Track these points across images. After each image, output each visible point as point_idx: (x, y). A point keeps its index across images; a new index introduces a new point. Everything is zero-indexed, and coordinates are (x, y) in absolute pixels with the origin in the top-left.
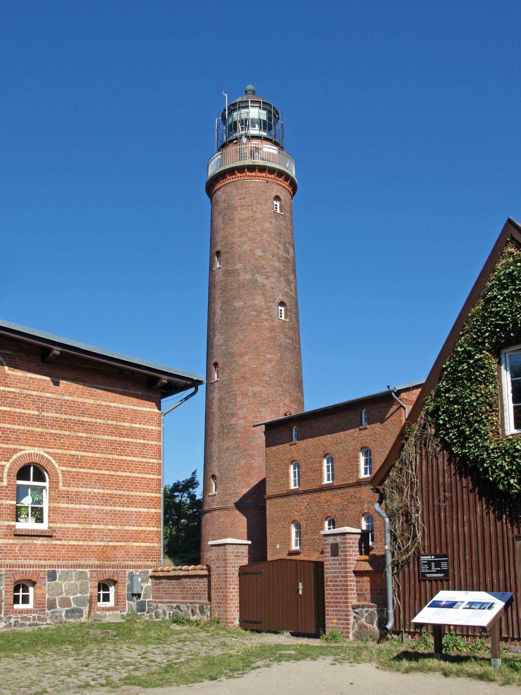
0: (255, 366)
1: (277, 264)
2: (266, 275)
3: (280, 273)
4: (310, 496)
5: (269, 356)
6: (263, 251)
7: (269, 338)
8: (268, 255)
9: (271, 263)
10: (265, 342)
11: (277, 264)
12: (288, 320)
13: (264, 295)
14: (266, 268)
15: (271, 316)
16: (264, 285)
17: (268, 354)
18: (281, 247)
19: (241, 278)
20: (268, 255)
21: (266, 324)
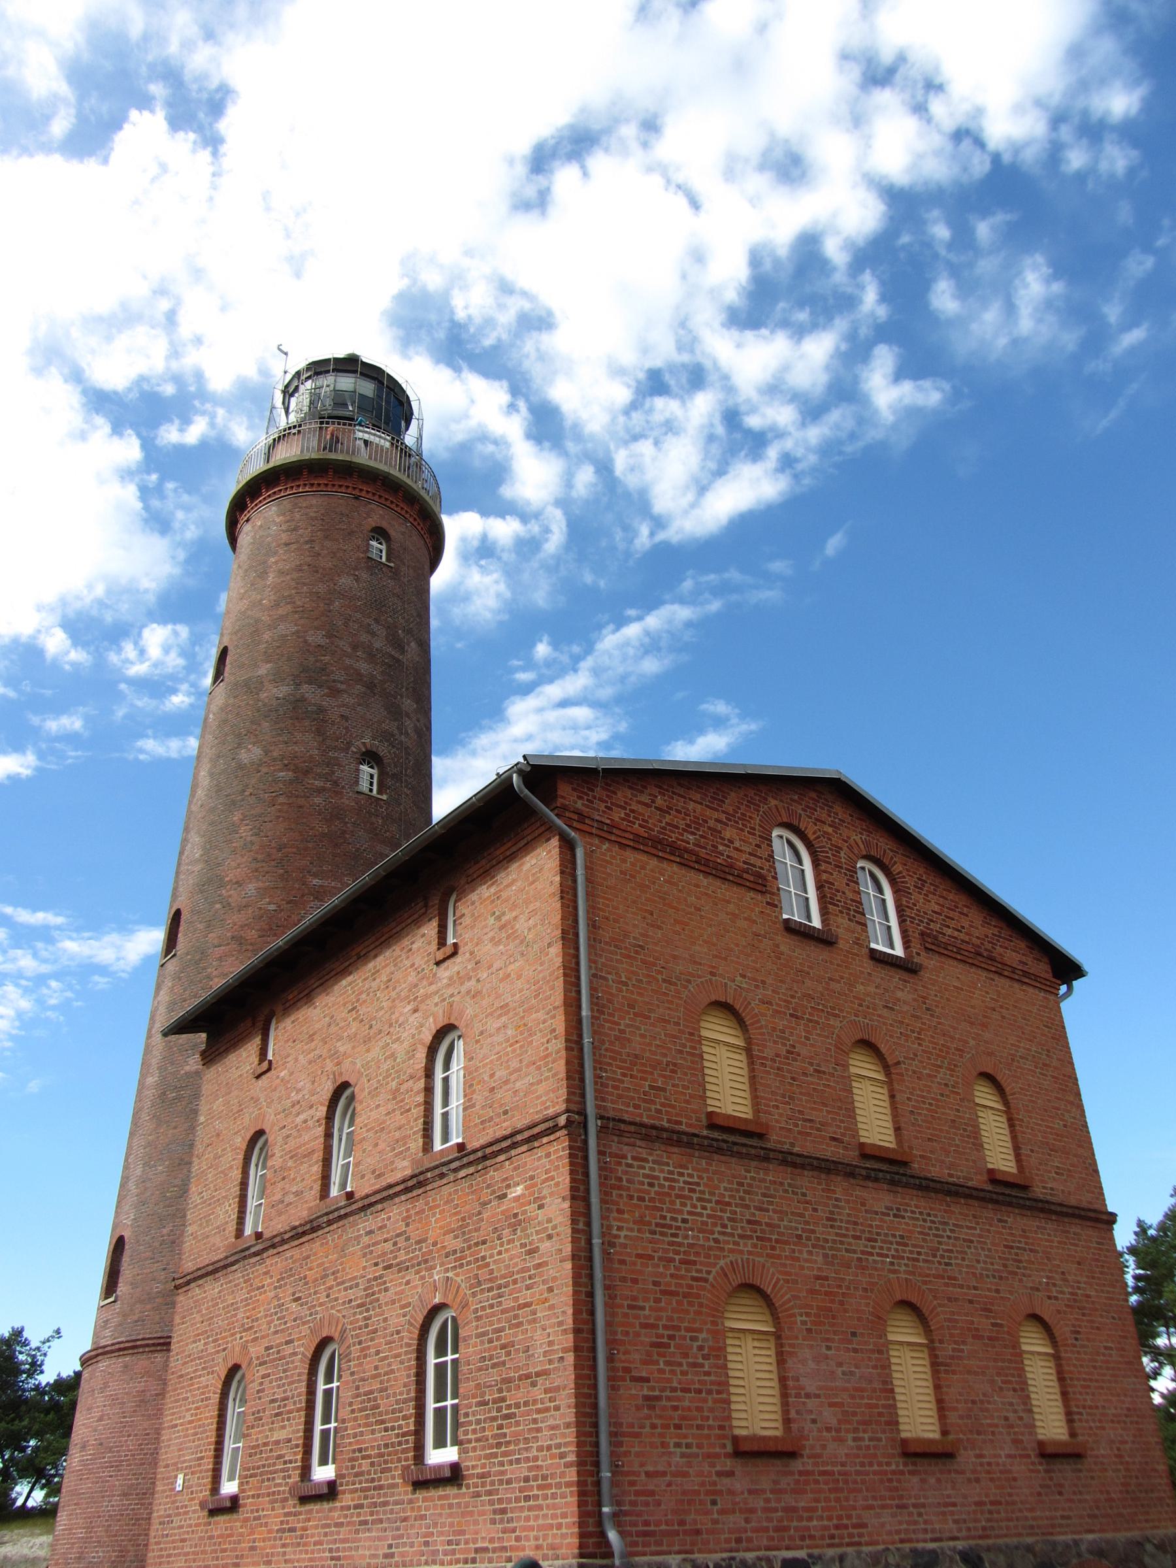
0: (272, 907)
1: (364, 667)
2: (329, 688)
3: (371, 686)
4: (275, 1263)
5: (315, 881)
6: (329, 635)
7: (323, 835)
8: (341, 643)
9: (347, 661)
10: (310, 845)
11: (364, 667)
12: (384, 797)
13: (319, 732)
14: (333, 672)
15: (336, 783)
16: (321, 710)
17: (315, 875)
18: (382, 632)
19: (263, 695)
20: (341, 643)
21: (317, 800)
